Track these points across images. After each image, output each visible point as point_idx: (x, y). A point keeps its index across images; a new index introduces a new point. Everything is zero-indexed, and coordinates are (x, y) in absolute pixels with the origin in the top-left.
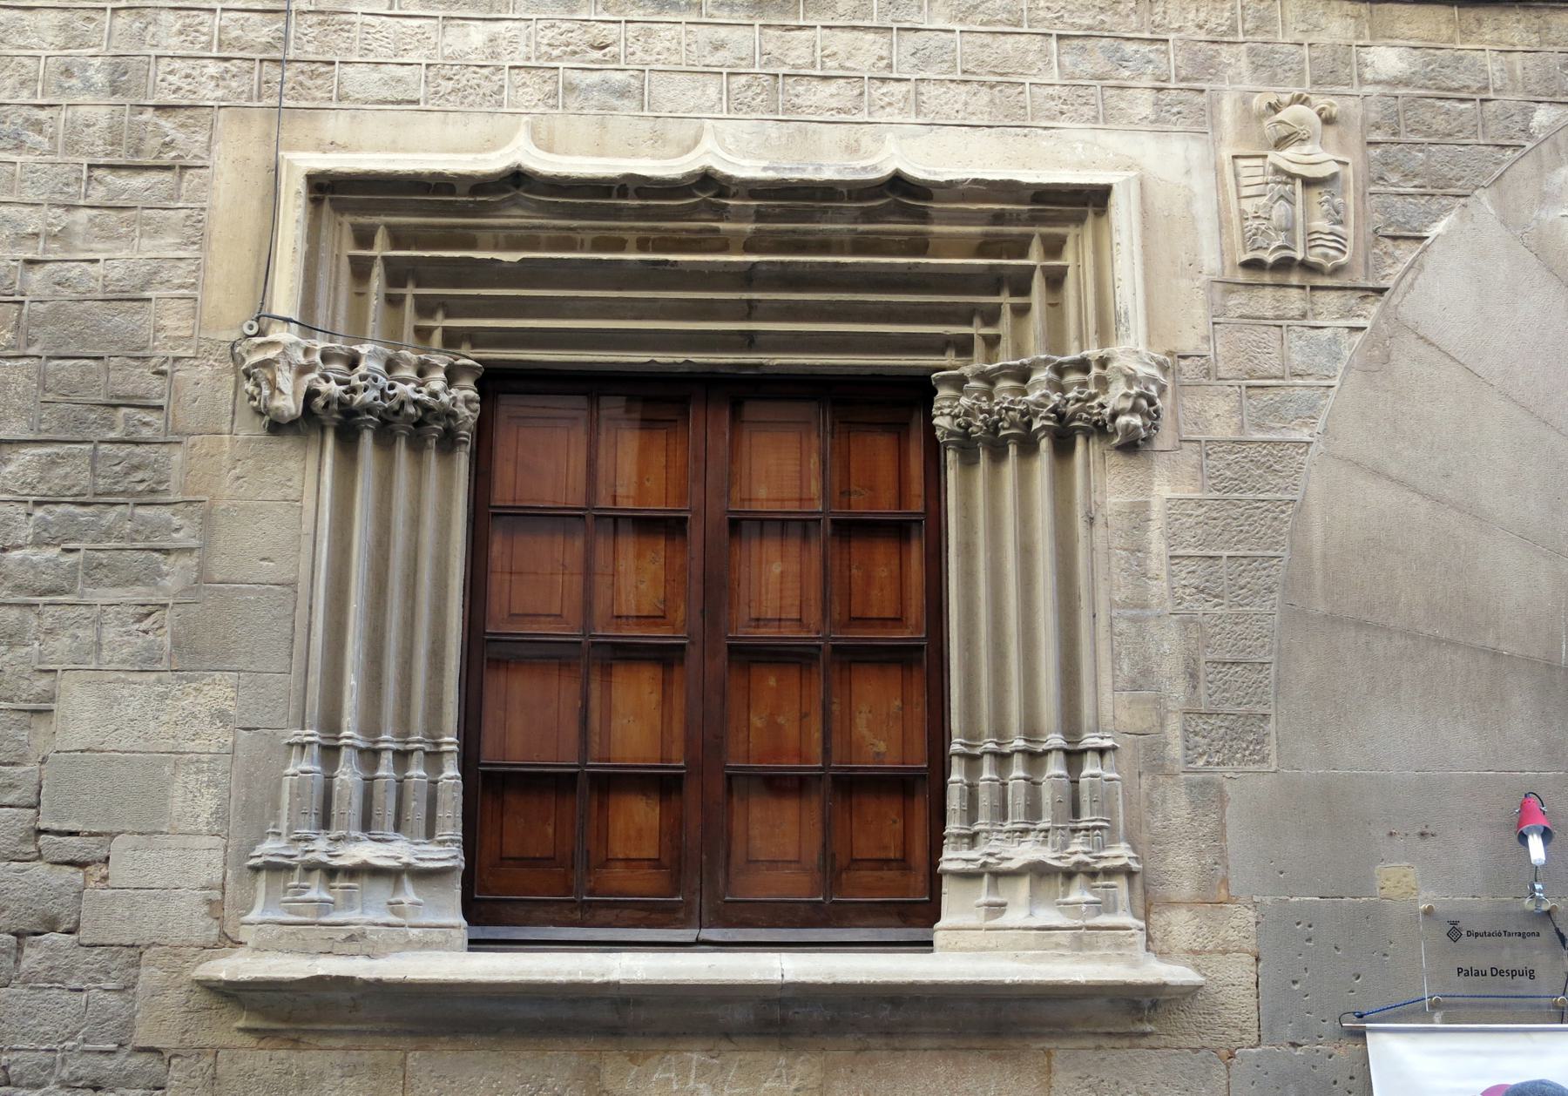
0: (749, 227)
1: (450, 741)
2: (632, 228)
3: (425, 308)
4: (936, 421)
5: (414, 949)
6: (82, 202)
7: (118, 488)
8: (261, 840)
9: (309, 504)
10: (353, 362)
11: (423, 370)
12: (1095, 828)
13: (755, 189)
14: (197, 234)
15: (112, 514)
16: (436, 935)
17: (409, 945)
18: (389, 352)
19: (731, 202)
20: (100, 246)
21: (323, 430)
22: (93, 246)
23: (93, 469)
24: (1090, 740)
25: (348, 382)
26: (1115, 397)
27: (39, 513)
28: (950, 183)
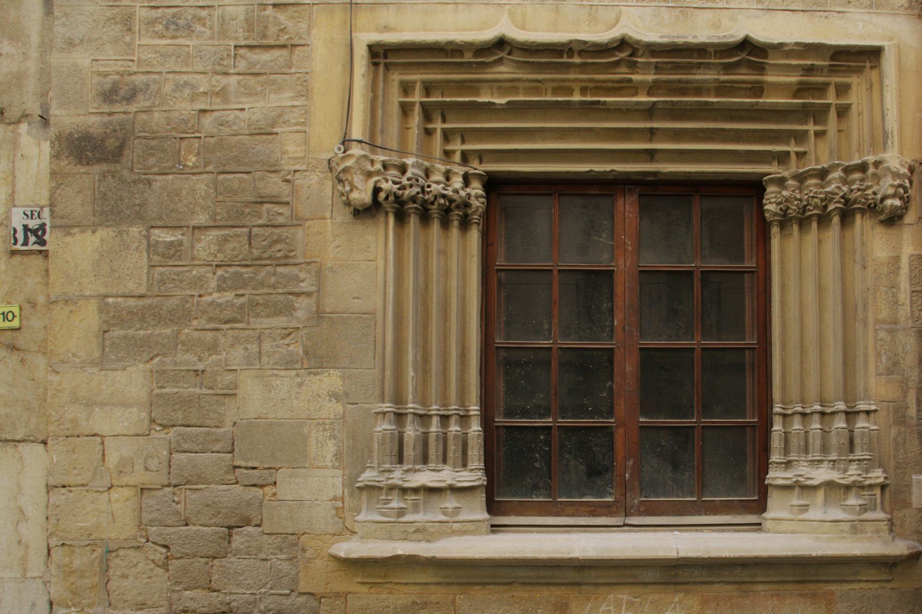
0: (650, 78)
1: (474, 409)
2: (577, 80)
3: (447, 136)
4: (766, 207)
5: (456, 535)
6: (232, 71)
7: (266, 255)
8: (363, 471)
9: (381, 263)
10: (403, 169)
11: (448, 176)
12: (864, 460)
13: (654, 49)
14: (305, 91)
15: (264, 272)
16: (470, 527)
17: (453, 533)
18: (426, 164)
19: (640, 60)
20: (245, 100)
21: (387, 213)
22: (242, 100)
23: (250, 244)
24: (862, 406)
25: (400, 183)
26: (887, 186)
27: (220, 272)
28: (781, 45)
